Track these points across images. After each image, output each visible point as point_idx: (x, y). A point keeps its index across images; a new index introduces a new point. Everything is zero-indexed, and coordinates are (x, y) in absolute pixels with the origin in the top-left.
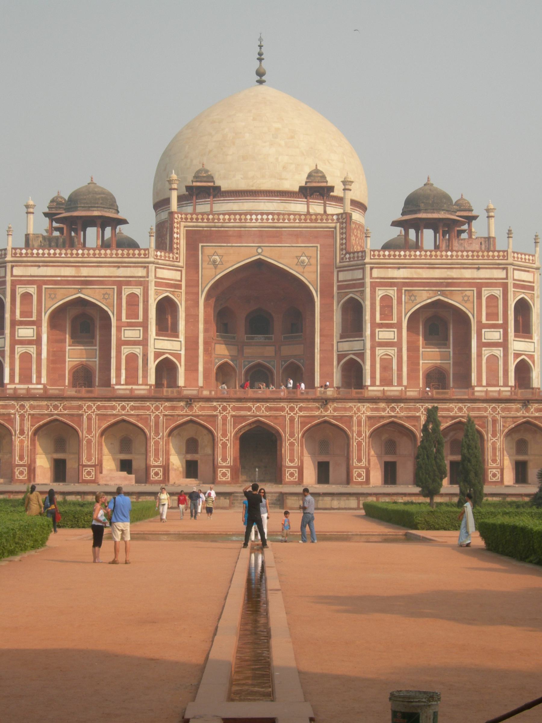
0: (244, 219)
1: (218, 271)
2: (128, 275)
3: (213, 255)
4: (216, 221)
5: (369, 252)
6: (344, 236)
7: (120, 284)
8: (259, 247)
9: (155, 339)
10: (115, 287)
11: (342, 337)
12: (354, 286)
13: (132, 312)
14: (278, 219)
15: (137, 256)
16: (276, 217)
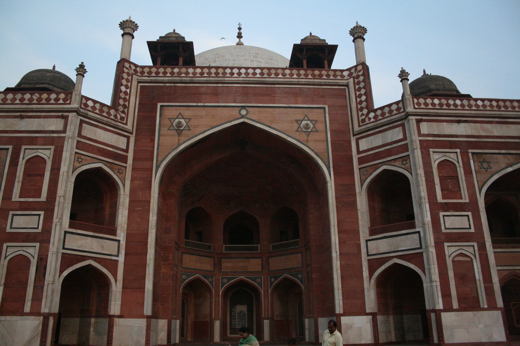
0: (222, 74)
1: (182, 139)
2: (34, 129)
3: (177, 118)
4: (183, 75)
5: (411, 99)
6: (363, 91)
7: (18, 142)
8: (243, 107)
9: (66, 232)
10: (11, 147)
11: (372, 232)
12: (389, 153)
13: (32, 186)
14: (269, 74)
15: (52, 101)
16: (266, 71)
